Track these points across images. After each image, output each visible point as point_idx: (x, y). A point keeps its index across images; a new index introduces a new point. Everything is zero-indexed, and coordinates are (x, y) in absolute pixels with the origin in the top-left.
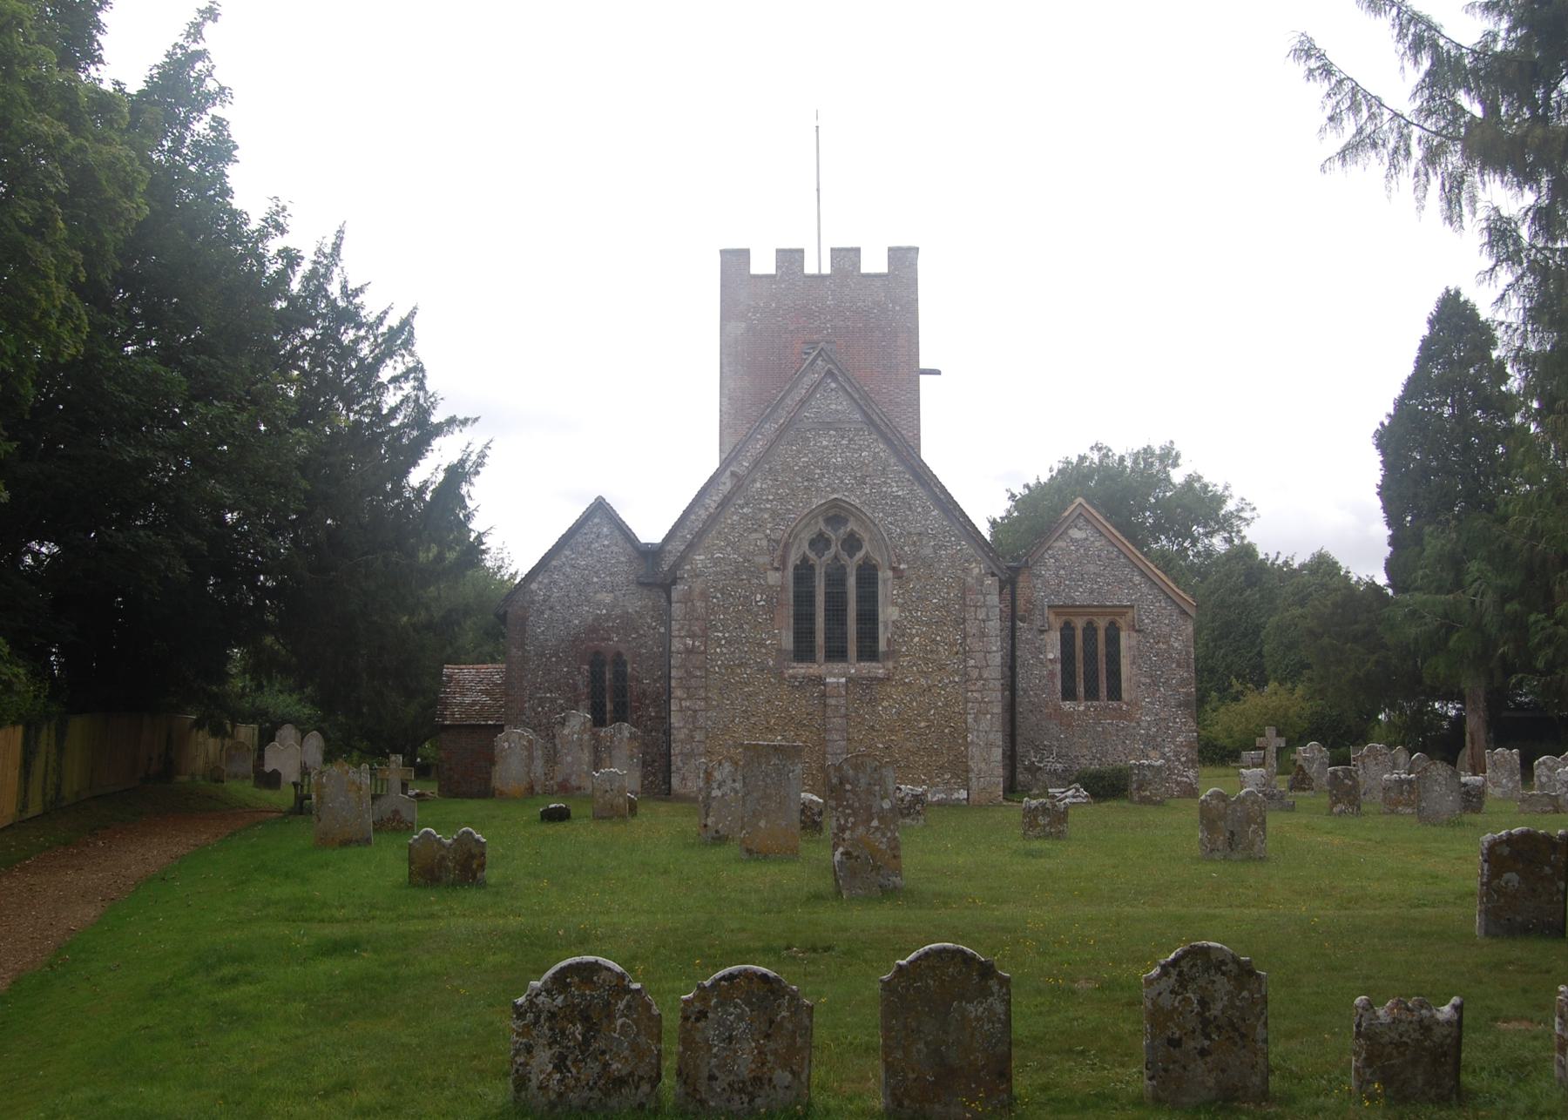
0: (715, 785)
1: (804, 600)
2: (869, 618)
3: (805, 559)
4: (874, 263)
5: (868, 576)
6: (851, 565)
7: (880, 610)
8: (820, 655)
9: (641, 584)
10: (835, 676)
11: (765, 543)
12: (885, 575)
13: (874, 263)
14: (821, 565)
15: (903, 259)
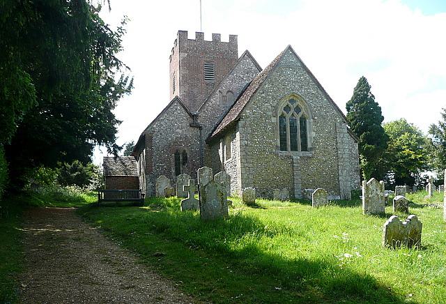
0: (370, 192)
1: (283, 128)
2: (304, 136)
3: (283, 114)
4: (225, 39)
5: (303, 120)
6: (298, 117)
7: (308, 133)
8: (289, 148)
9: (191, 126)
10: (297, 155)
11: (270, 107)
12: (310, 122)
13: (225, 39)
14: (288, 116)
15: (233, 38)
